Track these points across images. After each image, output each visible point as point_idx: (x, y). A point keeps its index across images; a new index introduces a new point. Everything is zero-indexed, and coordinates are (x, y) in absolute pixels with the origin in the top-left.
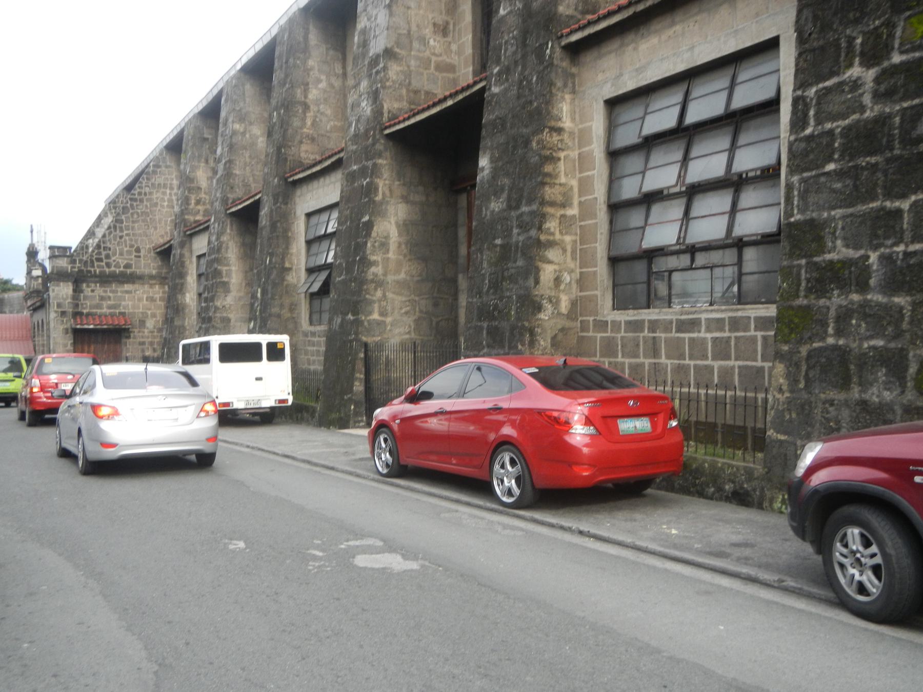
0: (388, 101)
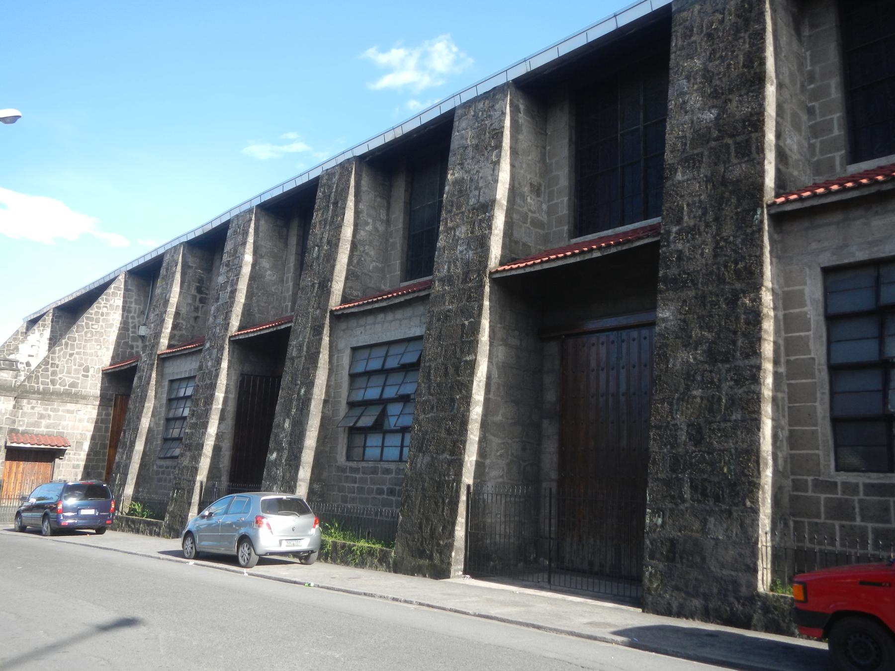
0: (496, 248)
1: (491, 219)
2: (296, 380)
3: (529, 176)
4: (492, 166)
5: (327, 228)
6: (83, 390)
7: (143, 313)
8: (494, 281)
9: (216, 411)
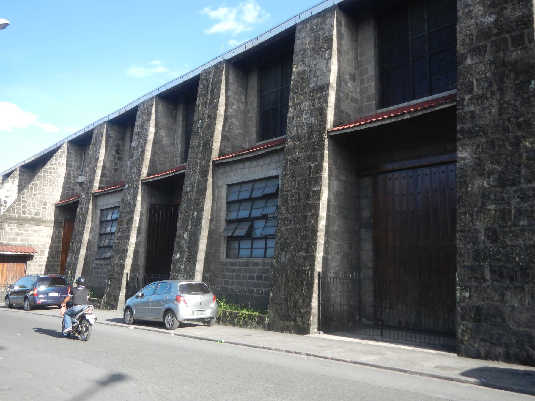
0: (330, 115)
1: (327, 96)
2: (190, 207)
3: (349, 69)
4: (325, 61)
5: (208, 107)
7: (79, 168)
8: (331, 137)
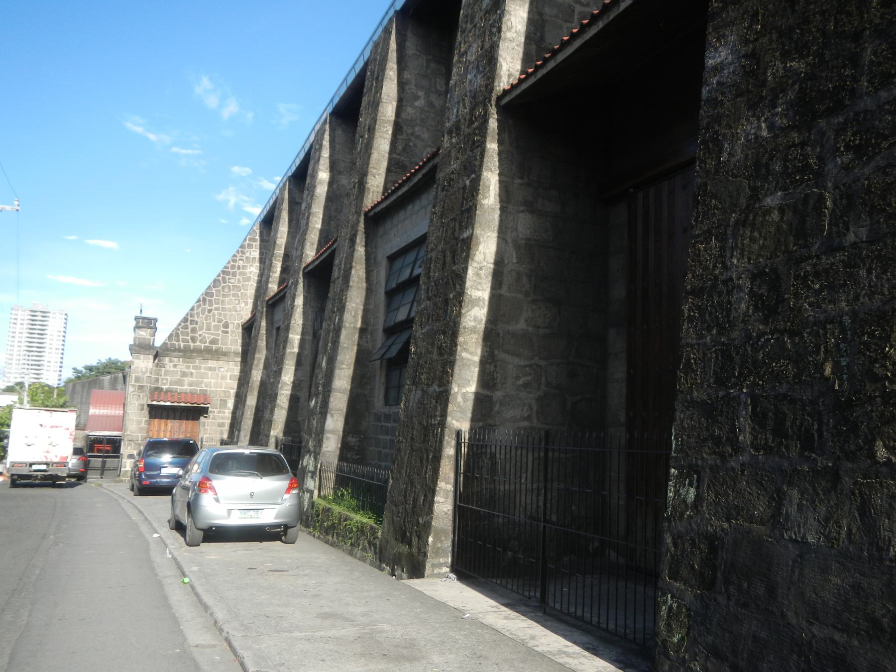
0: (509, 59)
6: (224, 347)
9: (292, 356)
